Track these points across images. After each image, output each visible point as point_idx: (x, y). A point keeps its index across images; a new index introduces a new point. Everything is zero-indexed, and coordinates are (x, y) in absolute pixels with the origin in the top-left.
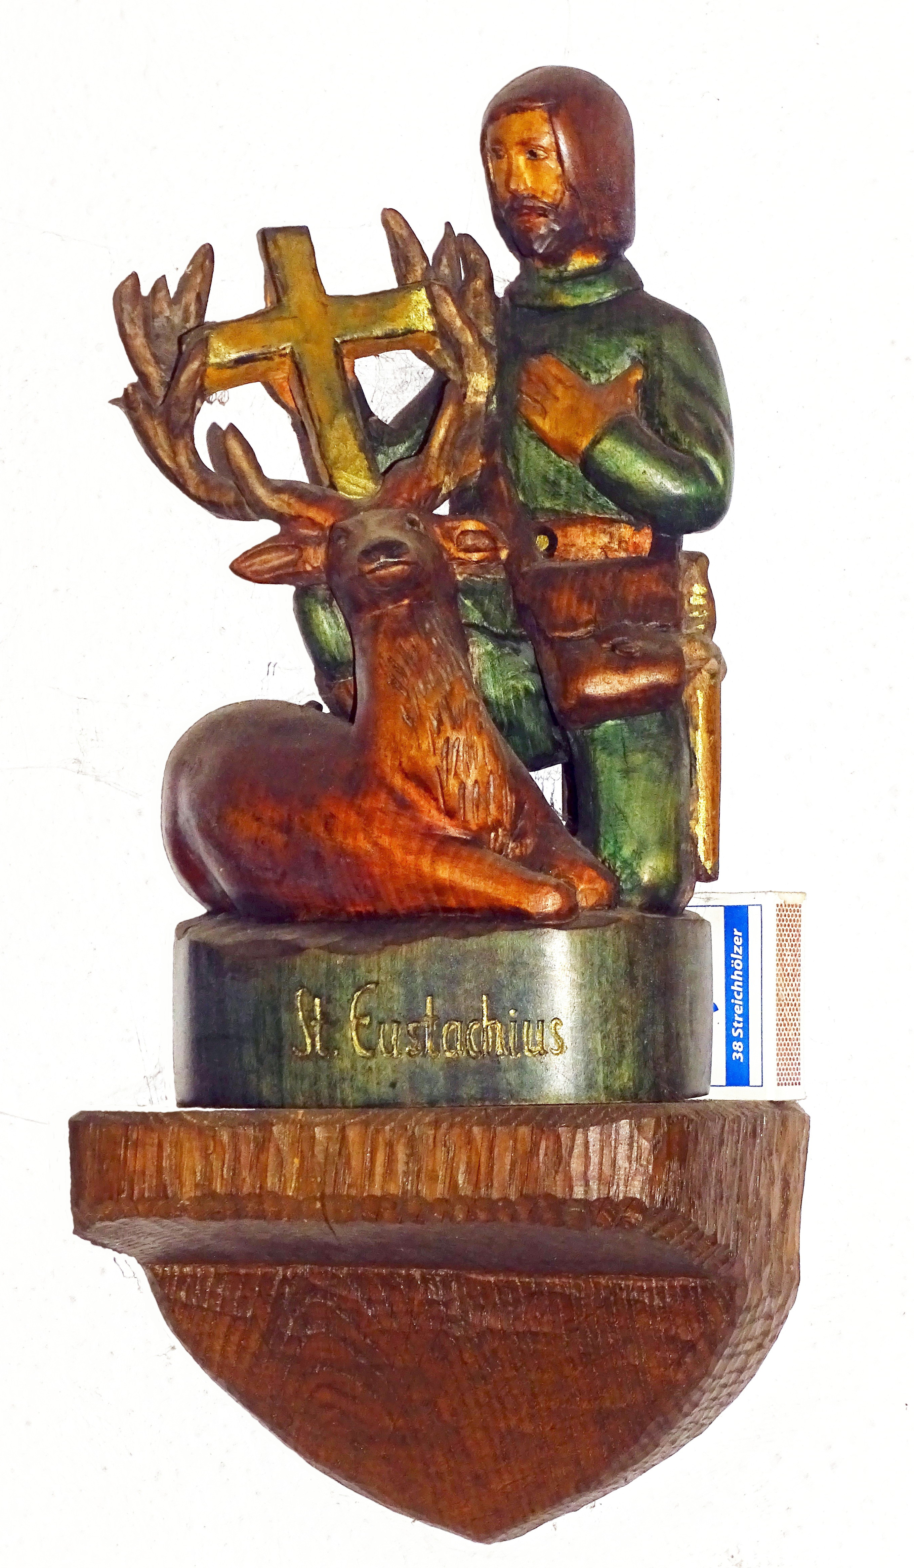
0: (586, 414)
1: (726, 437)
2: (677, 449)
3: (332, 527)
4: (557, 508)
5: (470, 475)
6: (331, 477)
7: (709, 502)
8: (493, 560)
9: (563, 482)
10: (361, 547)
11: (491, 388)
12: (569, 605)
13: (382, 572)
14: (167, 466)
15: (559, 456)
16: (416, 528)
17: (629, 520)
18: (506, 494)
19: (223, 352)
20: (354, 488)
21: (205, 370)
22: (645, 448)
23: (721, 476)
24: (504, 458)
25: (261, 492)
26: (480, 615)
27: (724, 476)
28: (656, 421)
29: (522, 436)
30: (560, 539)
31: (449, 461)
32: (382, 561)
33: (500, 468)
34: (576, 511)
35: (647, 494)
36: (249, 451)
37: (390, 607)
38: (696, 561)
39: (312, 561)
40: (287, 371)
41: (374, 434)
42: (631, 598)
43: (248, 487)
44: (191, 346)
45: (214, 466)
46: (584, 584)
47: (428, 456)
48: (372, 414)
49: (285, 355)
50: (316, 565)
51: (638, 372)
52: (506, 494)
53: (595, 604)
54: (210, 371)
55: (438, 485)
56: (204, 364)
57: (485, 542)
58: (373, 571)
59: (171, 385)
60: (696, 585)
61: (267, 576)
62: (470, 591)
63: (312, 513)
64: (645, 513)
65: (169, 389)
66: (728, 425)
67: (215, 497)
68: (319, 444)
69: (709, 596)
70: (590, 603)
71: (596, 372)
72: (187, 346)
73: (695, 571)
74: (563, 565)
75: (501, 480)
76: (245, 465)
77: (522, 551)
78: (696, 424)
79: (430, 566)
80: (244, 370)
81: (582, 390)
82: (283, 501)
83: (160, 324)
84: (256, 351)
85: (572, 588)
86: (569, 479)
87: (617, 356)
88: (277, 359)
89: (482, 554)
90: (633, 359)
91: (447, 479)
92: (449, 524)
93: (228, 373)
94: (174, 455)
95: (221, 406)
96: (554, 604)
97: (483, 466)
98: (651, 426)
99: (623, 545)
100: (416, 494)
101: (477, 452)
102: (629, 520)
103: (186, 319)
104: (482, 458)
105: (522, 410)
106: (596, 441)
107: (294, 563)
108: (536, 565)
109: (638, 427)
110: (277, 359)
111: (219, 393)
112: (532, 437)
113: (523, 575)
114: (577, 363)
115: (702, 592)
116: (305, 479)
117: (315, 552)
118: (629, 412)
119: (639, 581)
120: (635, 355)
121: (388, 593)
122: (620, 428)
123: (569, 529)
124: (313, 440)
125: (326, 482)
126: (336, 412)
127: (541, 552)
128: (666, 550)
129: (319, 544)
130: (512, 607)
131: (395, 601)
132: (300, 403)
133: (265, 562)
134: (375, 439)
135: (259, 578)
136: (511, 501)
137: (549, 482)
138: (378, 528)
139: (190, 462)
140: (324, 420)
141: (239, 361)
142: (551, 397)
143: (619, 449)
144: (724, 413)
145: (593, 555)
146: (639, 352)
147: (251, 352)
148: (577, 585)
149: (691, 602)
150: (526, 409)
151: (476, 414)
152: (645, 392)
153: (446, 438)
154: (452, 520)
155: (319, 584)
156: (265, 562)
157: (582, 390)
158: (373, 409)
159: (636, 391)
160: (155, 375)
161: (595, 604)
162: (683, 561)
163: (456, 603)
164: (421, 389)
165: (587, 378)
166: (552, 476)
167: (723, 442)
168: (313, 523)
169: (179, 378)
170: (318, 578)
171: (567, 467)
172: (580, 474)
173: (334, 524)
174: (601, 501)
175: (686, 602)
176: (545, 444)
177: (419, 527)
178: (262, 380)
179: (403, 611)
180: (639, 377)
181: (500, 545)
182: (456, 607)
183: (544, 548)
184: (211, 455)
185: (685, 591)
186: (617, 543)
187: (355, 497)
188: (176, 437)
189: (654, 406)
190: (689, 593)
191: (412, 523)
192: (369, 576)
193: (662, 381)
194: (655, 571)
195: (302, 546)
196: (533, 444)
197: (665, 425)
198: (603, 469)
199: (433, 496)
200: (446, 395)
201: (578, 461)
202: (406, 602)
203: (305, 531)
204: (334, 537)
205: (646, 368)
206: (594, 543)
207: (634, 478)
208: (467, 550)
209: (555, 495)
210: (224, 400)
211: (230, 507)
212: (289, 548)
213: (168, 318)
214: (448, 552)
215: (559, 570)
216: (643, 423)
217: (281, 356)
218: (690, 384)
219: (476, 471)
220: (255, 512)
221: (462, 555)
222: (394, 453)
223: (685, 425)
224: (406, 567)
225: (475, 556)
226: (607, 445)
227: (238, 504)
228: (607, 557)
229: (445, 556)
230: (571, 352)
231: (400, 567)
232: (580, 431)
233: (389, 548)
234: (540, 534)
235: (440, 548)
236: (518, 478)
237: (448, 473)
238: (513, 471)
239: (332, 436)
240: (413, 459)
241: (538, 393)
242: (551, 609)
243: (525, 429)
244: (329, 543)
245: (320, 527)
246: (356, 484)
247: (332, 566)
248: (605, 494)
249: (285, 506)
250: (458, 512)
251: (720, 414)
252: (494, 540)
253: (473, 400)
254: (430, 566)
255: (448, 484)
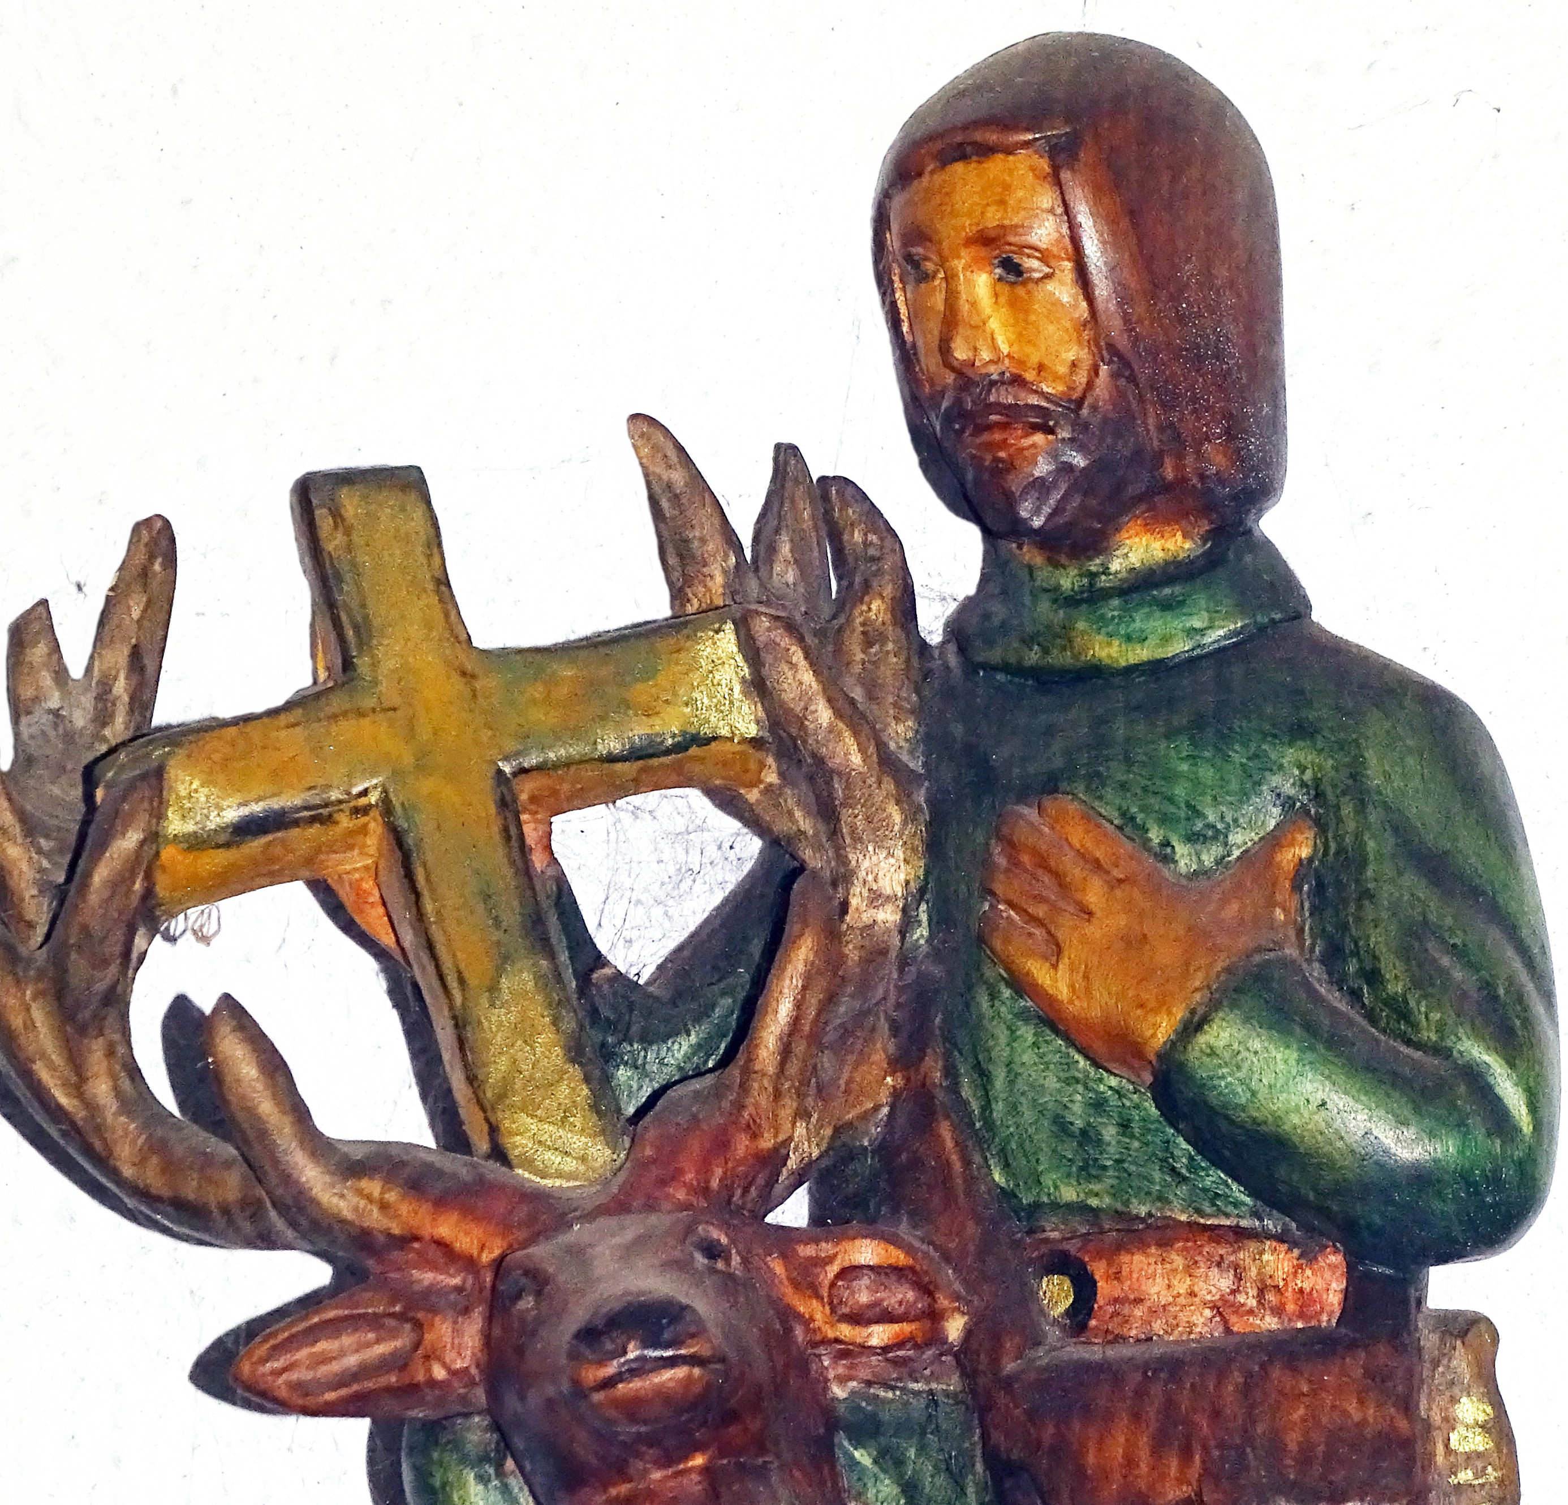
0: (1166, 954)
1: (1539, 1009)
2: (1408, 1042)
3: (499, 1265)
4: (1094, 1202)
5: (865, 1117)
6: (494, 1130)
7: (1495, 1180)
8: (928, 1344)
9: (1110, 1133)
10: (578, 1315)
11: (913, 886)
12: (1130, 1462)
13: (636, 1385)
14: (59, 1107)
15: (1096, 1065)
16: (720, 1265)
17: (1286, 1230)
18: (957, 1166)
19: (201, 803)
20: (554, 1159)
21: (157, 854)
22: (1324, 1040)
23: (1524, 1110)
24: (950, 1072)
25: (312, 1176)
26: (896, 1490)
27: (1533, 1108)
28: (1352, 967)
29: (997, 1012)
30: (1105, 1289)
31: (805, 1082)
32: (631, 1356)
33: (940, 1096)
34: (1143, 1210)
35: (1331, 1165)
36: (275, 1066)
37: (657, 1475)
38: (1463, 1334)
39: (449, 1356)
40: (372, 850)
41: (605, 1012)
42: (1293, 1440)
43: (276, 1162)
44: (117, 792)
45: (181, 1105)
46: (1170, 1404)
47: (747, 1071)
48: (599, 960)
49: (366, 810)
50: (459, 1365)
51: (1300, 837)
52: (957, 1166)
53: (1197, 1458)
54: (168, 853)
55: (776, 1149)
56: (153, 837)
57: (901, 1296)
58: (609, 1383)
59: (65, 895)
60: (1464, 1400)
61: (330, 1396)
62: (866, 1428)
63: (447, 1228)
64: (1323, 1212)
65: (61, 903)
66: (1535, 962)
67: (190, 1190)
68: (462, 1043)
69: (1499, 1428)
70: (1186, 1454)
71: (1193, 838)
72: (109, 786)
73: (1461, 1362)
74: (1111, 1353)
75: (946, 1132)
76: (266, 1107)
77: (1003, 1321)
78: (1458, 975)
79: (761, 1369)
80: (257, 850)
81: (1155, 887)
82: (369, 1198)
83: (34, 730)
84: (289, 799)
85: (1136, 1416)
86: (1125, 1126)
87: (1245, 796)
88: (345, 821)
89: (896, 1327)
90: (1288, 804)
91: (800, 1130)
92: (807, 1251)
93: (219, 859)
94: (78, 1086)
95: (201, 946)
96: (1091, 1459)
97: (896, 1094)
98: (1338, 981)
99: (1271, 1297)
100: (719, 1172)
101: (879, 1057)
102: (1286, 1230)
103: (103, 717)
104: (892, 1074)
105: (998, 945)
106: (1193, 1026)
107: (399, 1362)
108: (1042, 1357)
109: (1306, 984)
110: (345, 821)
111: (193, 913)
112: (1023, 1015)
113: (1008, 1384)
114: (1140, 818)
115: (1481, 1418)
116: (427, 1139)
117: (457, 1332)
118: (1279, 945)
119: (1314, 1393)
120: (1292, 792)
121: (651, 1441)
122: (1259, 989)
123: (1125, 1258)
124: (444, 1035)
125: (482, 1145)
126: (504, 960)
127: (1055, 1322)
128: (1382, 1304)
129: (466, 1311)
130: (979, 1467)
131: (667, 1460)
132: (408, 939)
133: (325, 1359)
134: (609, 1026)
135: (310, 1402)
136: (970, 1180)
137: (1071, 1135)
138: (621, 1266)
139: (118, 1092)
140: (473, 981)
141: (246, 829)
142: (1071, 909)
143: (1256, 1044)
144: (1529, 941)
145: (1191, 1325)
146: (1303, 784)
147: (276, 804)
148: (1152, 1412)
149: (1454, 1444)
150: (1007, 941)
151: (875, 954)
152: (1320, 888)
153: (795, 1022)
154: (817, 1241)
155: (467, 1415)
156: (325, 1359)
157: (1155, 887)
158: (602, 946)
159: (1296, 887)
160: (24, 866)
161: (1197, 1458)
162: (1429, 1340)
163: (832, 1460)
164: (730, 887)
165: (1165, 856)
166: (1077, 1116)
167: (1528, 1023)
168: (447, 1253)
169: (88, 875)
170: (463, 1399)
171: (1118, 1092)
172: (1154, 1111)
173: (502, 1257)
174: (1208, 1182)
175: (1440, 1448)
176: (1057, 1032)
177: (728, 1261)
178: (307, 874)
179: (694, 1485)
180: (1305, 852)
181: (943, 1302)
182: (835, 1476)
183: (1061, 1308)
184: (174, 1086)
185: (1436, 1418)
186: (1253, 1292)
187: (558, 1183)
188: (82, 1030)
189: (1344, 927)
190: (1446, 1419)
191: (712, 1251)
192: (598, 1397)
193: (1364, 863)
194: (1356, 1364)
195: (420, 1315)
196: (1027, 1033)
197: (1373, 977)
198: (1212, 1097)
199: (768, 1175)
200: (794, 910)
201: (1148, 1078)
202: (698, 1460)
203: (427, 1277)
204: (505, 1293)
205: (1321, 826)
206: (1192, 1294)
207: (1295, 1119)
208: (858, 1318)
209: (1089, 1171)
210: (209, 929)
211: (226, 1211)
212: (390, 1322)
213: (56, 713)
214: (807, 1322)
215: (1101, 1368)
216: (1316, 972)
217: (356, 811)
218: (1436, 867)
219: (877, 1108)
220: (293, 1224)
221: (845, 1331)
222: (661, 1063)
223: (1426, 979)
224: (697, 1371)
225: (879, 1335)
226: (1222, 1034)
227: (253, 1208)
228: (1228, 1330)
229: (799, 1332)
230: (1123, 786)
231: (680, 1372)
232: (1149, 996)
233: (651, 1320)
234: (1050, 1271)
235: (787, 1315)
236: (989, 1124)
237: (802, 1114)
238: (975, 1106)
239: (495, 1022)
240: (709, 1079)
241: (1040, 899)
242: (1080, 1472)
243: (1007, 993)
244: (492, 1308)
245: (469, 1264)
246: (561, 1148)
247: (504, 1363)
248: (1218, 1163)
249: (376, 1213)
250: (831, 1217)
251: (1523, 951)
252: (927, 1290)
253: (866, 918)
254: (761, 1369)
255: (805, 1143)
